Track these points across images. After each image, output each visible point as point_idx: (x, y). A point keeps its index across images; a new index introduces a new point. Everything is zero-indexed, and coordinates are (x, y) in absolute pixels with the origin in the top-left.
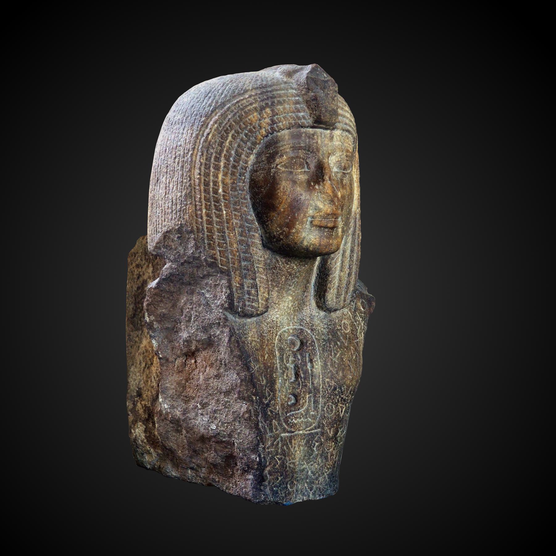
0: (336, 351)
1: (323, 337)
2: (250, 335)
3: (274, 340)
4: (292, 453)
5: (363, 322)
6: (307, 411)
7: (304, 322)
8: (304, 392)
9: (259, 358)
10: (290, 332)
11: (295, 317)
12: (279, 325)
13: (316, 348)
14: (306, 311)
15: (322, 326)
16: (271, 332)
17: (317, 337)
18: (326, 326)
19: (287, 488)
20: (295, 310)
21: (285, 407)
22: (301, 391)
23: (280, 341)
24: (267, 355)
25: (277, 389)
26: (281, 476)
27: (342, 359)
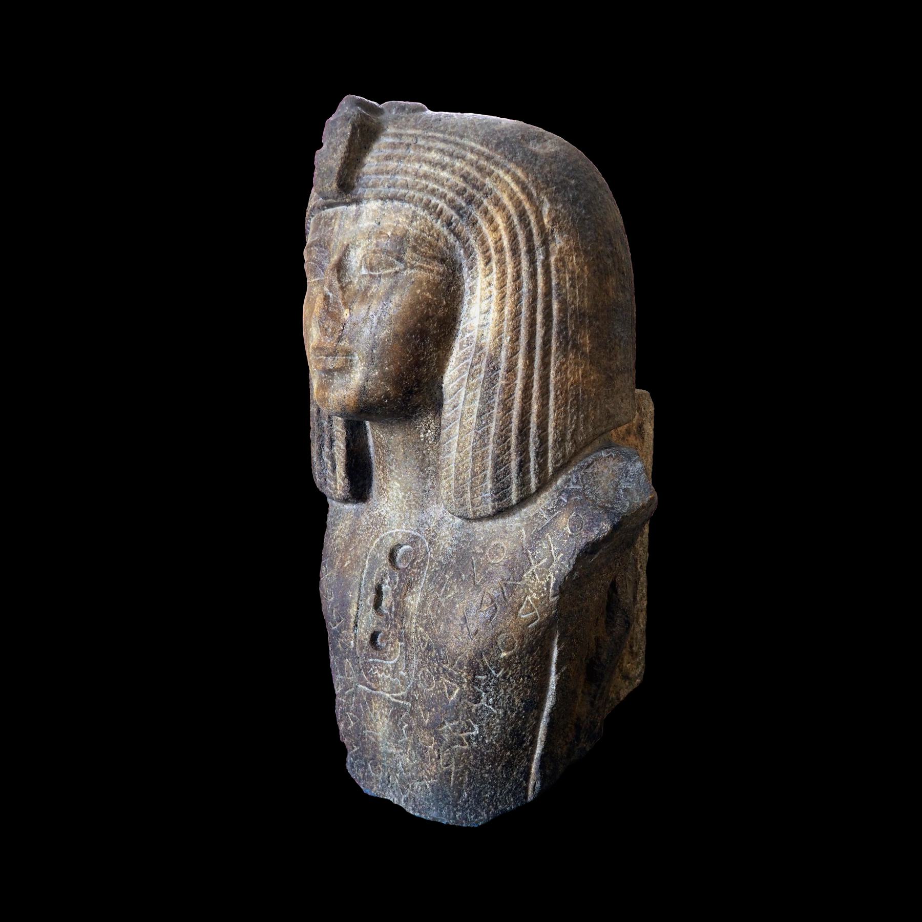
0: (450, 587)
1: (441, 558)
2: (340, 527)
3: (369, 544)
4: (371, 720)
5: (562, 555)
6: (395, 667)
7: (425, 527)
8: (393, 635)
9: (335, 563)
10: (397, 537)
11: (413, 516)
12: (386, 523)
13: (423, 573)
14: (436, 510)
15: (450, 542)
16: (371, 530)
17: (432, 556)
18: (456, 542)
19: (366, 767)
20: (410, 505)
21: (364, 646)
22: (390, 633)
23: (378, 546)
24: (349, 562)
25: (352, 615)
26: (357, 745)
27: (455, 603)
